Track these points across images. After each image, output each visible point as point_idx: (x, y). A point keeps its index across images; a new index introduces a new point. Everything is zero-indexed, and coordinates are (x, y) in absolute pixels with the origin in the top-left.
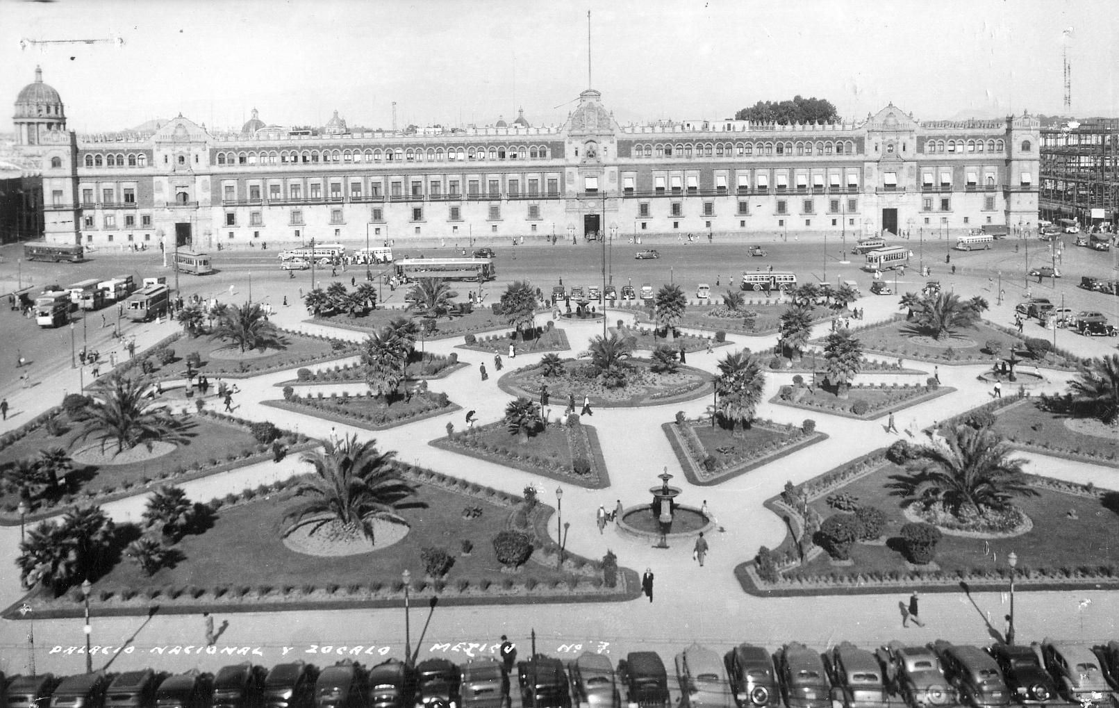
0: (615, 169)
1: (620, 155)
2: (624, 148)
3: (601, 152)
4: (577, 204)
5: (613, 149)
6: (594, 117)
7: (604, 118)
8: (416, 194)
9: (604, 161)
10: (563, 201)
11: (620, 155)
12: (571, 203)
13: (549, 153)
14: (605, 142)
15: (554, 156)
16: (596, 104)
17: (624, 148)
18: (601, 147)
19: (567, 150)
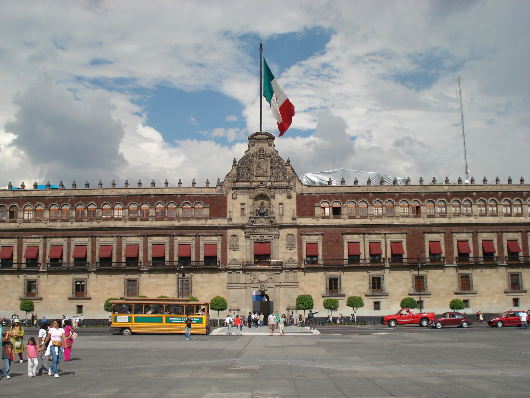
0: (294, 231)
1: (301, 213)
2: (307, 203)
3: (276, 210)
4: (243, 277)
5: (291, 205)
6: (266, 166)
7: (283, 171)
8: (33, 262)
9: (278, 221)
10: (224, 276)
11: (301, 213)
12: (234, 275)
13: (206, 211)
14: (280, 197)
15: (214, 215)
16: (269, 150)
17: (307, 203)
18: (275, 203)
19: (230, 207)
